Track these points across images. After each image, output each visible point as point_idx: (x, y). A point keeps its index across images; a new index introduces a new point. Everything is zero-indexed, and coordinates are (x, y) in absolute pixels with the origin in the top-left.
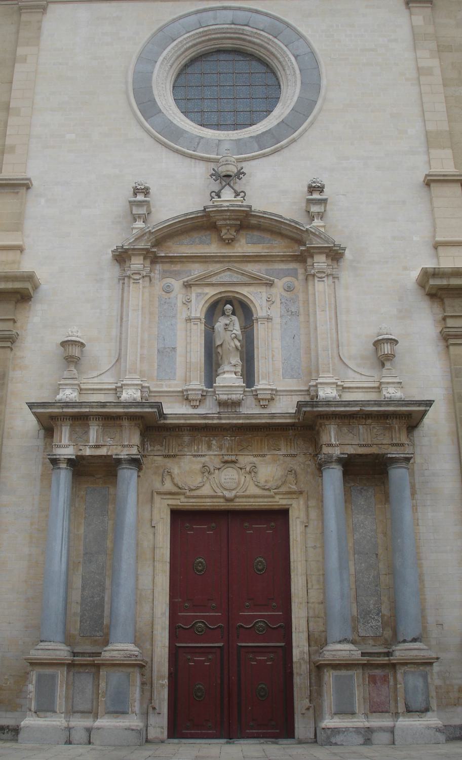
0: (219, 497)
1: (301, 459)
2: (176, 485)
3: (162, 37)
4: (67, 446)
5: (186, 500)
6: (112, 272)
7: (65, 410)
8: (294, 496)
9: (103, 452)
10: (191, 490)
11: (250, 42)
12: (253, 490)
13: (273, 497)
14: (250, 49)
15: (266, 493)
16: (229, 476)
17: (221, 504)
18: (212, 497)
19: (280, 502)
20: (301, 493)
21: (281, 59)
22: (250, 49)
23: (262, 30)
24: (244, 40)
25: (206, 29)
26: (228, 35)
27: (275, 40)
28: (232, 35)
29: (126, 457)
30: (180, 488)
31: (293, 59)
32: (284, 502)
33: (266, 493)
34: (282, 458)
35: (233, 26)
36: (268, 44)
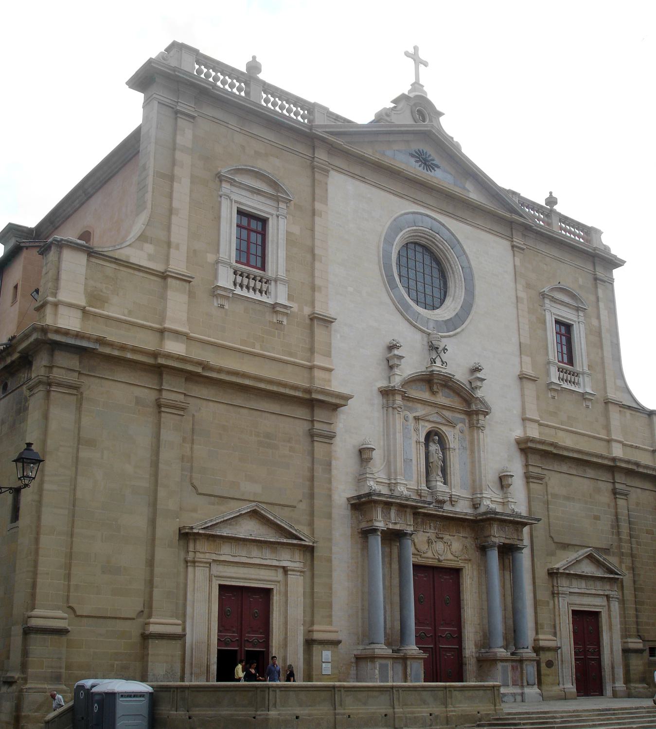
0: (435, 559)
1: (469, 540)
2: (417, 549)
3: (395, 228)
4: (380, 521)
5: (420, 559)
6: (378, 400)
7: (388, 499)
8: (467, 562)
9: (397, 527)
10: (424, 553)
11: (436, 245)
12: (450, 557)
13: (458, 561)
14: (434, 250)
15: (456, 559)
16: (439, 546)
17: (435, 563)
18: (433, 559)
19: (460, 564)
20: (470, 560)
21: (453, 266)
22: (434, 249)
23: (446, 241)
24: (434, 243)
25: (417, 228)
26: (426, 236)
27: (452, 250)
28: (428, 237)
29: (410, 532)
30: (419, 552)
31: (460, 268)
32: (462, 565)
33: (456, 559)
34: (461, 538)
35: (431, 231)
36: (447, 251)
